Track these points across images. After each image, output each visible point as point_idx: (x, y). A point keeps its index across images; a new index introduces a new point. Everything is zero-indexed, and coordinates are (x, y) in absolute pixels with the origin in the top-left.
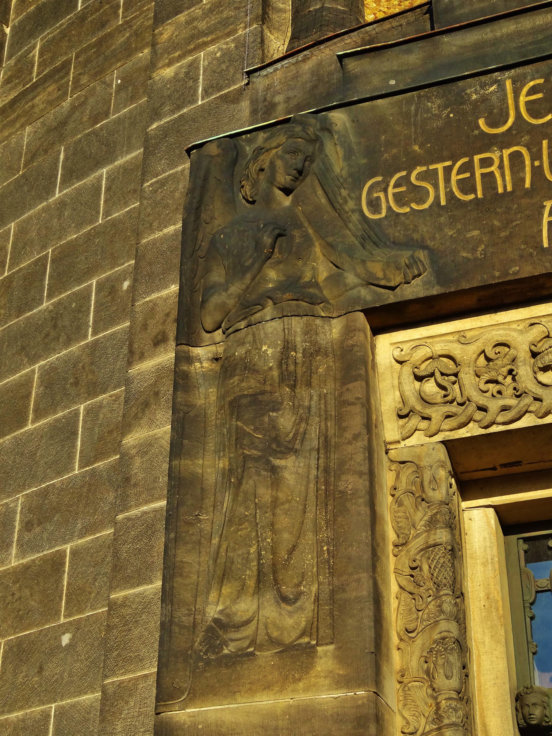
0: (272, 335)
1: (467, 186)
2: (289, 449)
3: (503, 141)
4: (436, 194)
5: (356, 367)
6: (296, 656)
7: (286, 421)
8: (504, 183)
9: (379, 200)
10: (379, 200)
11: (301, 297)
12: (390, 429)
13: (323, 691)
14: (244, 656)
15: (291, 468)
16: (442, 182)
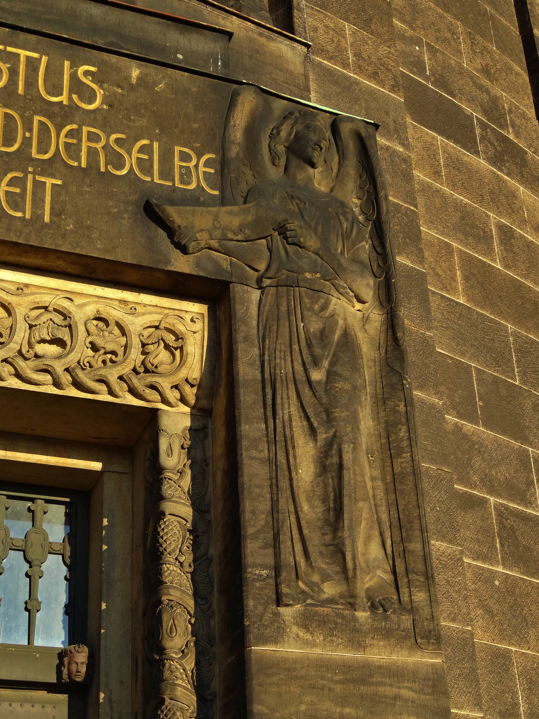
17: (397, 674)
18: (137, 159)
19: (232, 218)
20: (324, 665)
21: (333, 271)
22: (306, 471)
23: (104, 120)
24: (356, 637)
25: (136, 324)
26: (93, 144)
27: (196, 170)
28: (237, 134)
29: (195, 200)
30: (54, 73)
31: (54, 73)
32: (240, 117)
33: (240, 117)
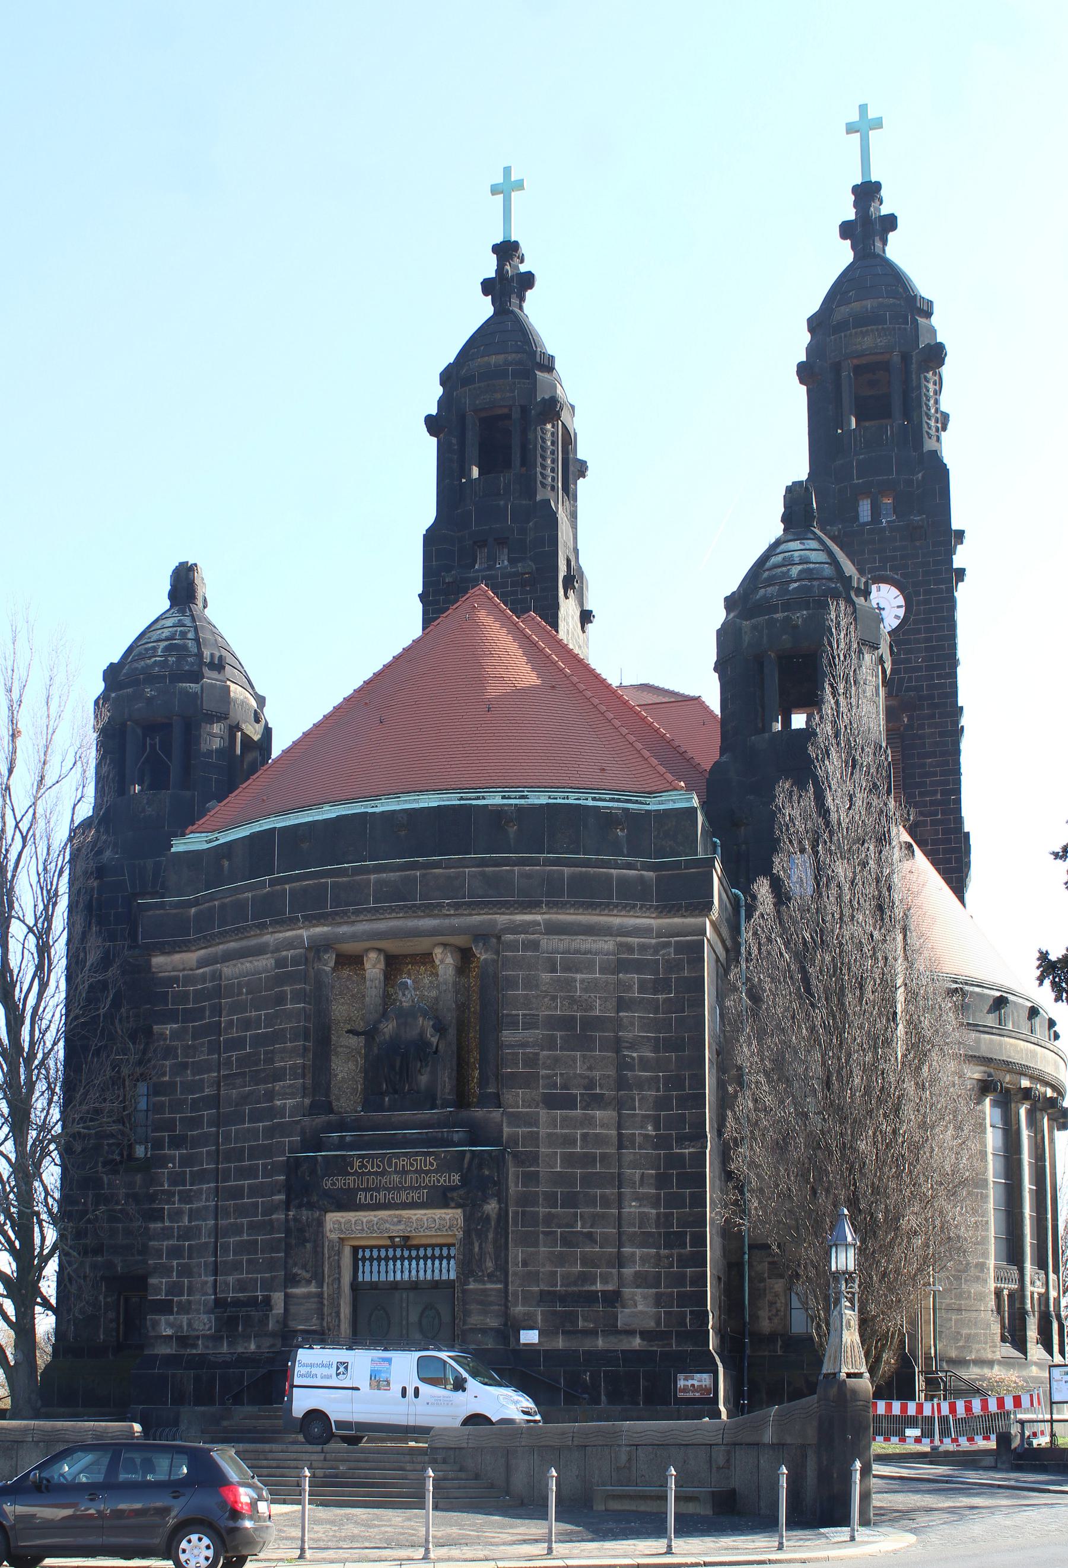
0: (305, 1214)
1: (345, 1184)
2: (308, 1241)
3: (352, 1174)
4: (339, 1185)
5: (320, 1223)
6: (309, 1282)
7: (307, 1235)
8: (352, 1186)
9: (327, 1184)
10: (327, 1184)
11: (311, 1206)
12: (328, 1234)
13: (313, 1289)
14: (299, 1281)
15: (308, 1245)
16: (340, 1182)
17: (491, 1289)
18: (443, 1180)
19: (462, 1192)
20: (477, 1289)
21: (485, 1200)
22: (477, 1249)
23: (436, 1171)
24: (484, 1282)
25: (448, 1217)
26: (433, 1179)
27: (456, 1178)
28: (466, 1166)
29: (454, 1188)
30: (425, 1161)
31: (425, 1161)
32: (466, 1161)
33: (466, 1161)
